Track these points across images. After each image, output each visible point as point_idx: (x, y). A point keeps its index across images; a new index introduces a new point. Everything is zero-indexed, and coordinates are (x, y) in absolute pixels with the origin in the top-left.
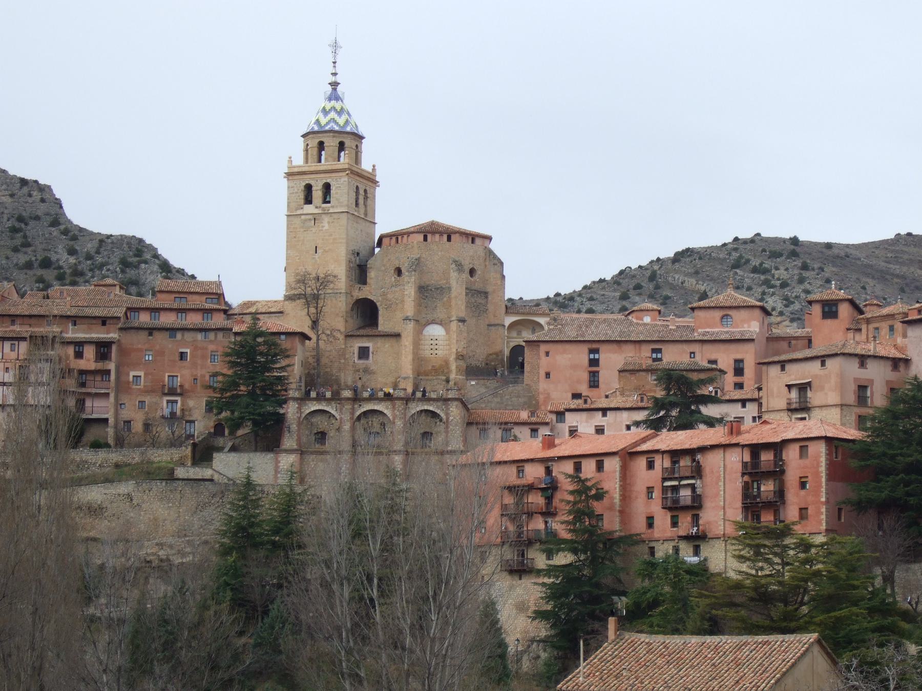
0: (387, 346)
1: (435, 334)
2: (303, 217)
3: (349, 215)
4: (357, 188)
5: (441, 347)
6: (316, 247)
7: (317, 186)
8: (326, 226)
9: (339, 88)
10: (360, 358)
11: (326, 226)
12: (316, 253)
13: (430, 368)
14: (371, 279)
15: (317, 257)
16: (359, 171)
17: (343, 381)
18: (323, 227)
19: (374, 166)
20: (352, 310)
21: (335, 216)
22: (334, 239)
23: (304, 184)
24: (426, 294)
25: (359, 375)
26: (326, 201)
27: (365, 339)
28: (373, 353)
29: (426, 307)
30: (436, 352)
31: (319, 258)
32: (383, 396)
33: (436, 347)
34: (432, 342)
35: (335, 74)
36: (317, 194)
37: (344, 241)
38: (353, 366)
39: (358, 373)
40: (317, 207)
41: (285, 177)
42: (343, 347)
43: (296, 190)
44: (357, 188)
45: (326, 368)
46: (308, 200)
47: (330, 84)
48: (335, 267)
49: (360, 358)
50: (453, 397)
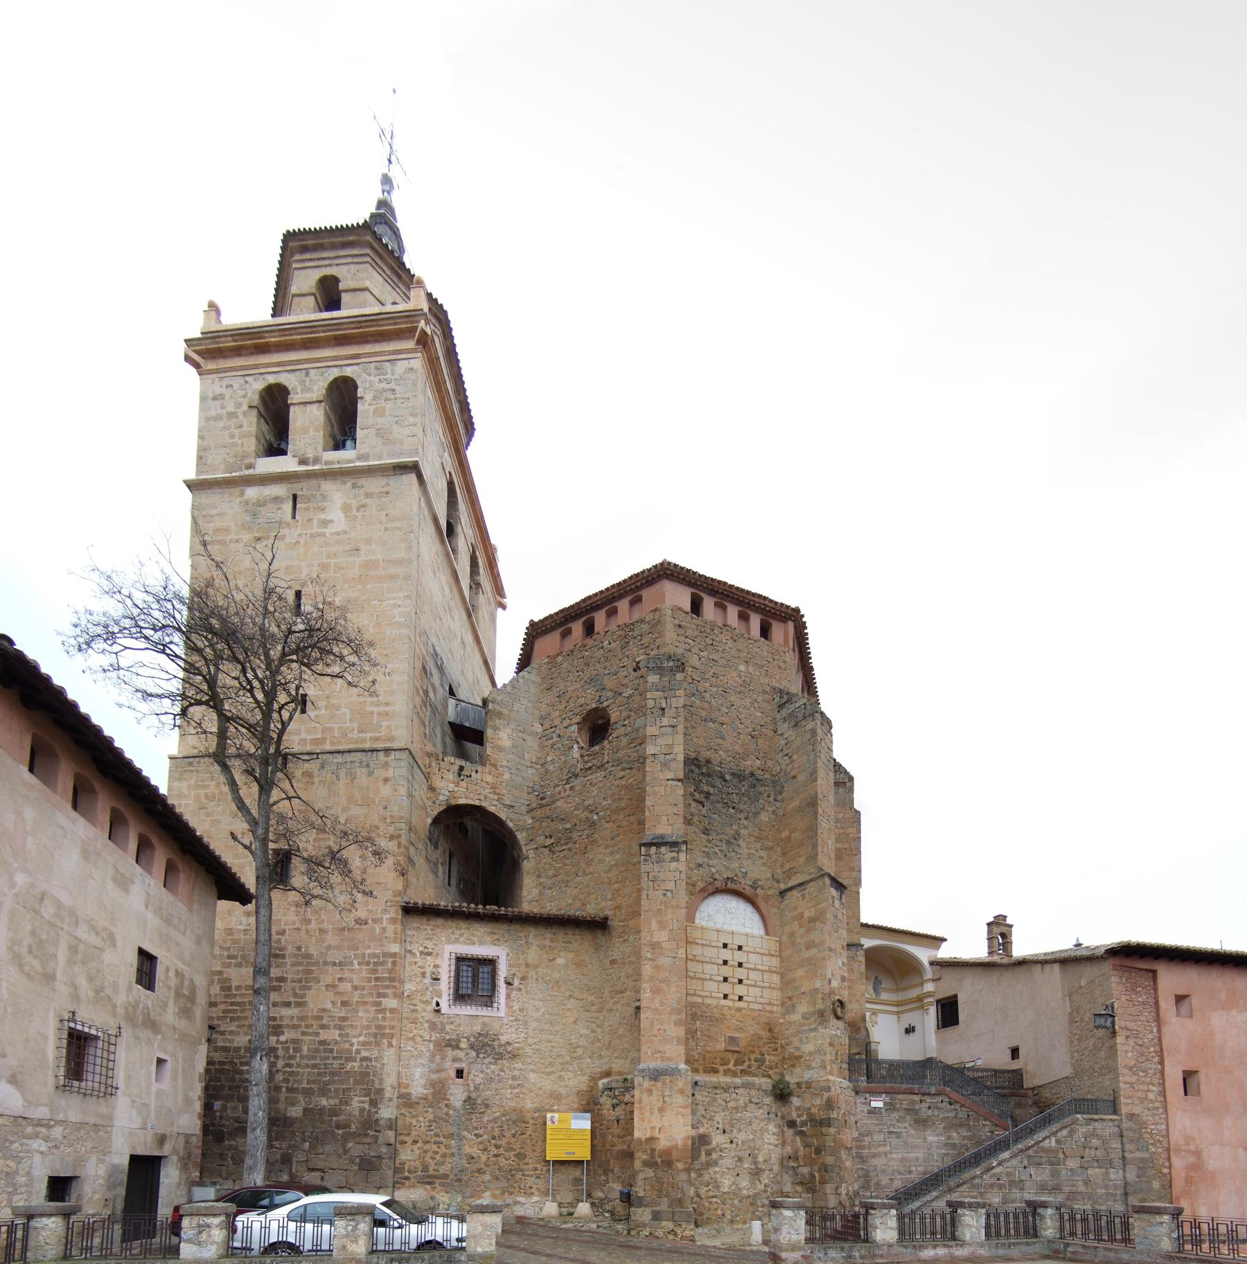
0: (560, 961)
1: (735, 929)
5: (754, 976)
10: (460, 997)
13: (721, 1046)
17: (390, 1081)
18: (325, 523)
22: (370, 565)
24: (706, 788)
25: (455, 1060)
27: (480, 929)
28: (508, 984)
29: (706, 832)
30: (740, 990)
33: (741, 973)
34: (726, 955)
38: (433, 1027)
39: (450, 1053)
42: (395, 948)
49: (460, 997)
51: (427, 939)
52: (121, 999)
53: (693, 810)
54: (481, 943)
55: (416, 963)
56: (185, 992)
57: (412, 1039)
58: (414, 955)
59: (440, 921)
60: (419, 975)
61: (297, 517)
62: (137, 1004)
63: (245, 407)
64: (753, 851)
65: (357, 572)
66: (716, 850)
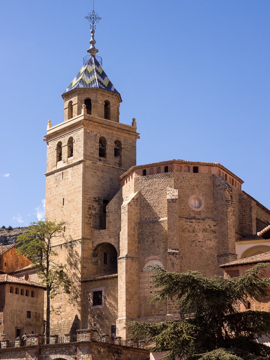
2: (56, 174)
6: (64, 199)
7: (65, 142)
8: (70, 176)
9: (97, 55)
11: (70, 176)
12: (63, 205)
14: (110, 222)
15: (64, 208)
16: (120, 127)
18: (68, 179)
19: (134, 120)
20: (95, 255)
21: (75, 167)
22: (75, 189)
23: (57, 143)
26: (71, 154)
31: (65, 209)
32: (19, 346)
35: (93, 43)
36: (65, 150)
37: (81, 189)
40: (64, 162)
41: (44, 140)
43: (52, 151)
45: (69, 316)
46: (59, 158)
47: (88, 51)
48: (75, 216)
50: (84, 340)
51: (87, 289)
52: (24, 322)
53: (141, 238)
54: (99, 287)
55: (85, 296)
56: (37, 316)
57: (85, 317)
58: (85, 293)
59: (90, 283)
60: (86, 299)
61: (63, 179)
62: (27, 321)
63: (54, 150)
64: (159, 245)
65: (73, 191)
66: (148, 248)
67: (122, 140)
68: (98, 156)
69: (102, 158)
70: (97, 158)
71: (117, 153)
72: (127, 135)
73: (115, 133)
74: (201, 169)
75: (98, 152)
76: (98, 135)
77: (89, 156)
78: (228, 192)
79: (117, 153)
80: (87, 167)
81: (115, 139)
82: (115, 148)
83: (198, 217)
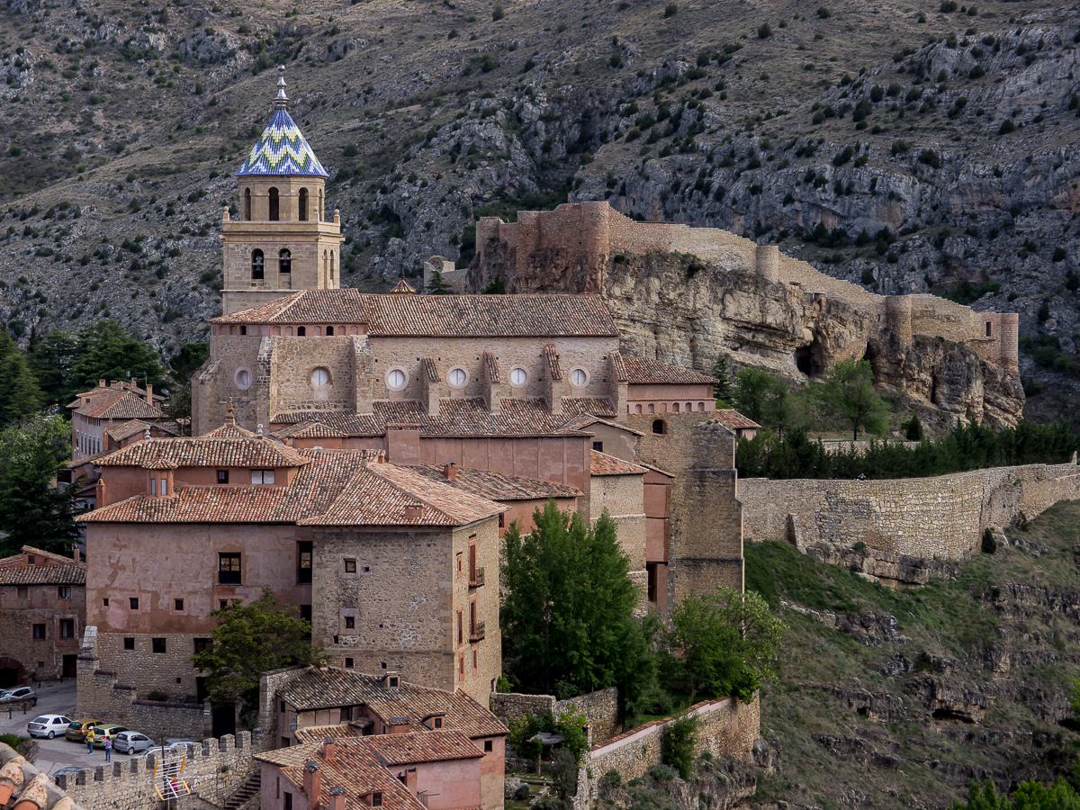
3: (230, 296)
4: (258, 253)
44: (258, 253)
67: (292, 248)
68: (250, 280)
69: (258, 281)
70: (248, 283)
71: (285, 268)
72: (300, 239)
73: (278, 239)
74: (250, 330)
75: (250, 274)
76: (251, 249)
77: (234, 283)
78: (261, 367)
79: (285, 268)
80: (231, 300)
81: (278, 248)
82: (281, 262)
83: (244, 398)
